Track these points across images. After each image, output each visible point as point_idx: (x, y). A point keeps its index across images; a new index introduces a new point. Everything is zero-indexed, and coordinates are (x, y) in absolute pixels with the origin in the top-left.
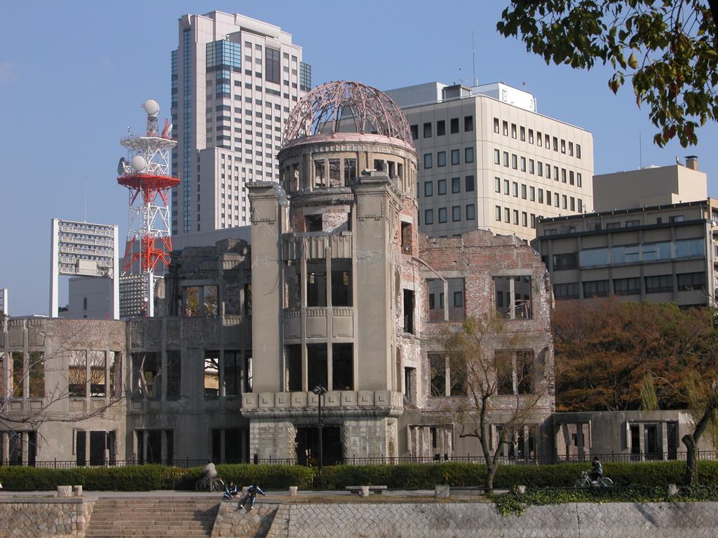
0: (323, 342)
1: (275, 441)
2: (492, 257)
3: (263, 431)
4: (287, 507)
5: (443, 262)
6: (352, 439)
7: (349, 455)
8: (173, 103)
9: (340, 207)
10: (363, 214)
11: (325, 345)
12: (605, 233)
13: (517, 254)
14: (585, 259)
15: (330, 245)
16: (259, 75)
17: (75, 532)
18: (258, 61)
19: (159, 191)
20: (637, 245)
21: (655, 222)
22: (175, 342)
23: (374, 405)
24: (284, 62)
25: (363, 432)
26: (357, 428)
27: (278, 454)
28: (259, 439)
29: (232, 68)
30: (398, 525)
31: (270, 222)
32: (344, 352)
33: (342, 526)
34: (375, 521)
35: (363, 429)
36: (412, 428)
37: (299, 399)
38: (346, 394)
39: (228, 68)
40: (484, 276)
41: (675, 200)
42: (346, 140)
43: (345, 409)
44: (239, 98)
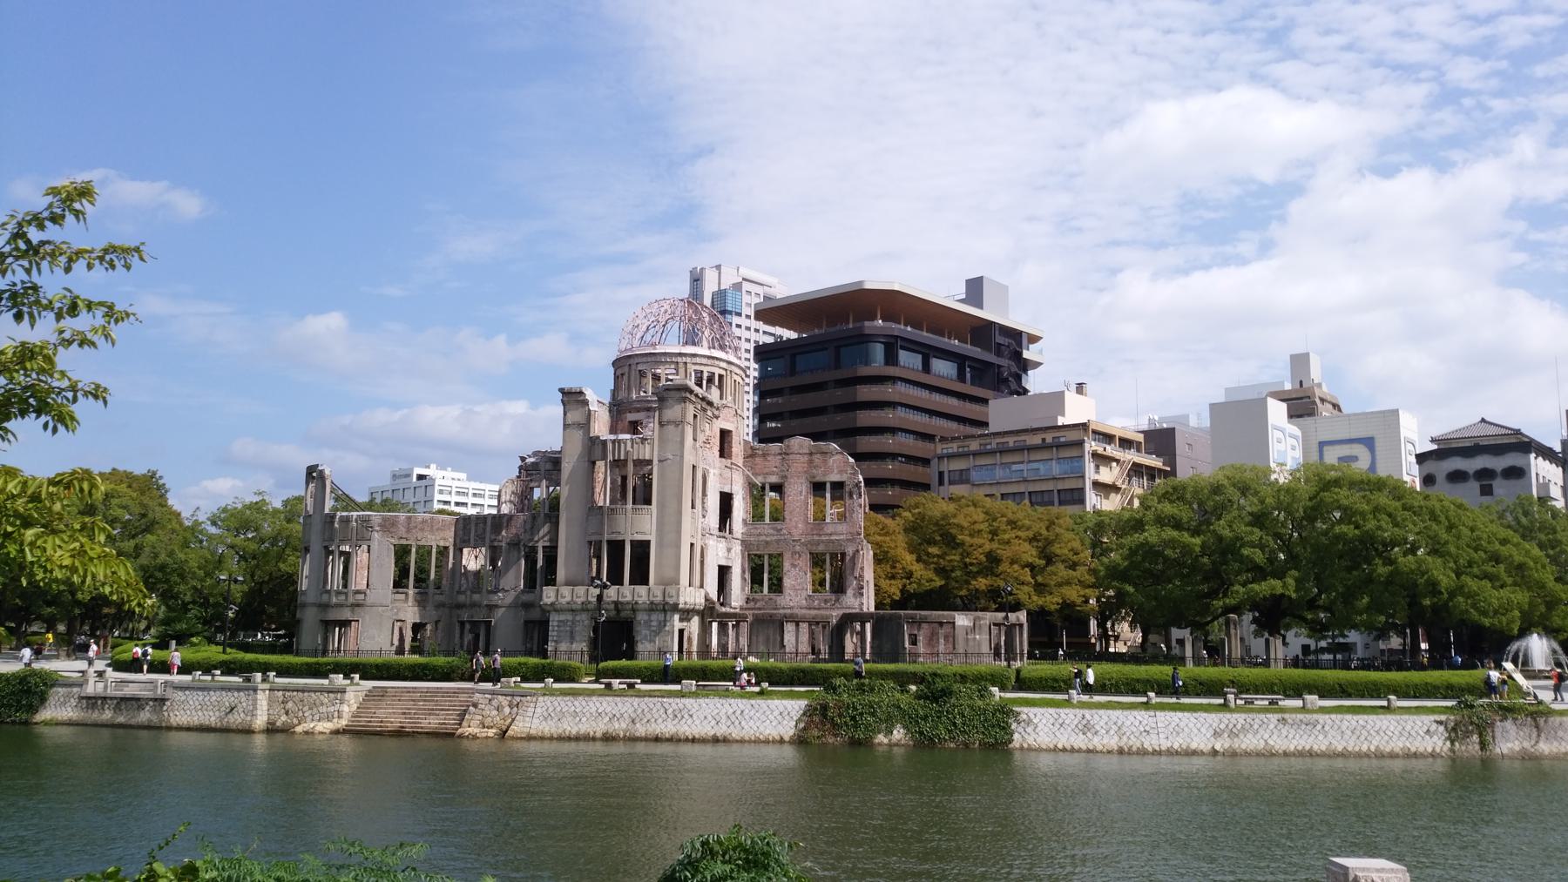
1: (572, 633)
2: (811, 462)
4: (534, 699)
6: (644, 632)
12: (992, 453)
15: (632, 447)
17: (336, 720)
20: (1022, 462)
21: (1040, 442)
26: (648, 623)
32: (641, 549)
35: (654, 623)
36: (711, 623)
39: (730, 313)
41: (1061, 421)
43: (636, 603)
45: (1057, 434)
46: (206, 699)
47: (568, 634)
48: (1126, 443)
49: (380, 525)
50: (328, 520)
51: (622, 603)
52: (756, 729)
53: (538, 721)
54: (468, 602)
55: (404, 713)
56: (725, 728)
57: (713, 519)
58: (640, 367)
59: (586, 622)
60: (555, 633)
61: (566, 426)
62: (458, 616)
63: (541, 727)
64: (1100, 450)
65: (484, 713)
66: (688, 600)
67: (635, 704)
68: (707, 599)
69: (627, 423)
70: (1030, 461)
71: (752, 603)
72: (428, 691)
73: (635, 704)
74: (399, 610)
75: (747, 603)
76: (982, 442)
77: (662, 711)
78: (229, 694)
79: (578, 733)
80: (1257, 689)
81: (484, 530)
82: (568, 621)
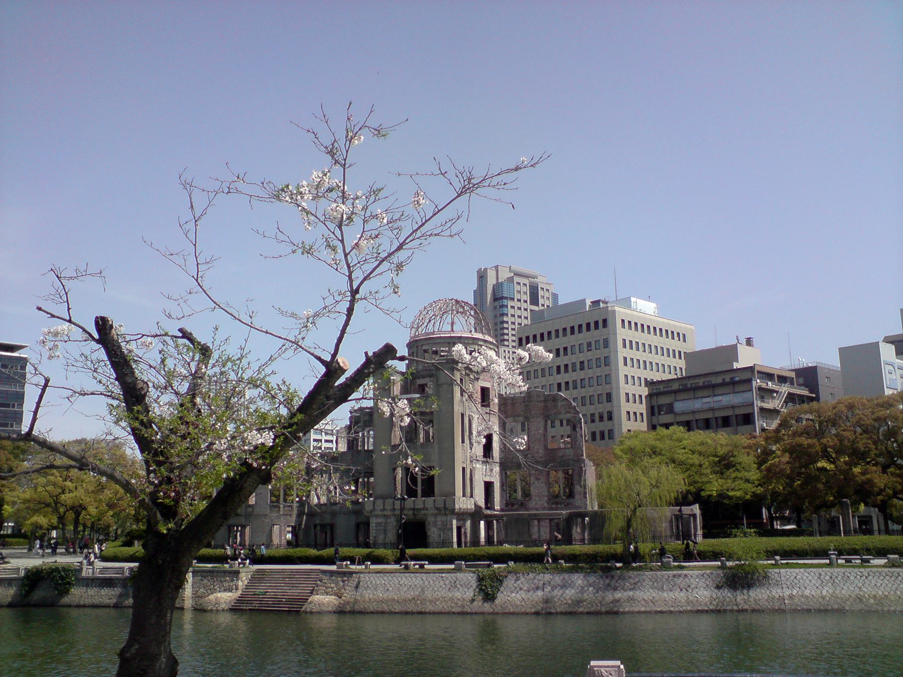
7: (431, 540)
13: (562, 406)
14: (679, 406)
16: (526, 301)
24: (541, 293)
26: (435, 524)
27: (387, 539)
28: (376, 530)
30: (426, 589)
33: (390, 589)
35: (439, 523)
39: (506, 298)
40: (540, 420)
41: (736, 366)
43: (427, 509)
44: (513, 316)
45: (732, 375)
47: (383, 531)
48: (783, 379)
57: (479, 450)
58: (425, 347)
64: (764, 385)
66: (461, 506)
68: (476, 505)
69: (417, 386)
70: (714, 396)
72: (292, 571)
73: (424, 578)
75: (506, 506)
77: (442, 583)
80: (855, 552)
82: (382, 523)
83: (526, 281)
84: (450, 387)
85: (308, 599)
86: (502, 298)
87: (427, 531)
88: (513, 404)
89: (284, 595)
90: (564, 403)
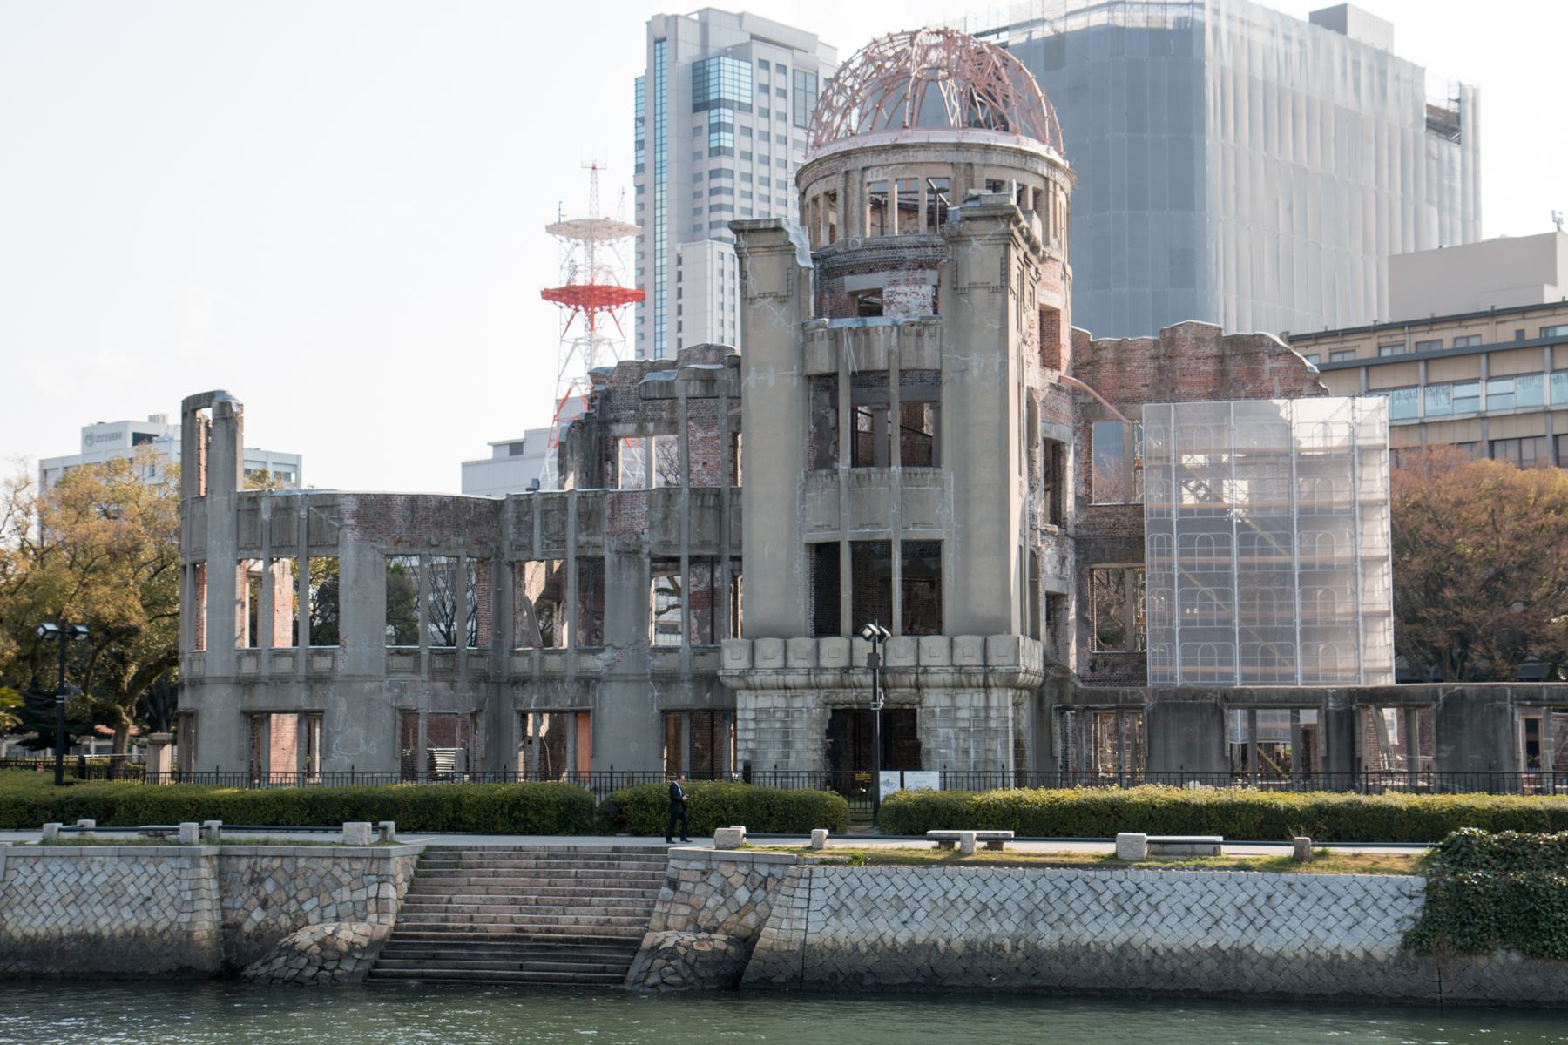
0: (882, 537)
3: (764, 716)
5: (1122, 387)
6: (941, 731)
8: (637, 166)
9: (918, 274)
10: (964, 283)
11: (887, 544)
13: (1273, 371)
17: (373, 918)
18: (782, 93)
19: (610, 311)
20: (1475, 381)
22: (598, 539)
23: (985, 666)
25: (963, 719)
27: (792, 760)
29: (736, 106)
31: (781, 300)
34: (990, 904)
37: (834, 649)
38: (928, 641)
39: (730, 104)
41: (1551, 296)
42: (932, 140)
43: (926, 671)
45: (1550, 321)
46: (84, 881)
47: (778, 736)
49: (356, 515)
50: (245, 505)
51: (893, 670)
52: (1306, 935)
53: (820, 917)
54: (536, 673)
55: (515, 902)
56: (1234, 934)
59: (816, 712)
60: (750, 735)
61: (747, 299)
62: (516, 701)
63: (829, 930)
65: (693, 901)
67: (1027, 882)
69: (845, 296)
70: (1490, 379)
71: (1107, 671)
73: (1027, 882)
74: (403, 689)
75: (1093, 669)
76: (1383, 340)
77: (1088, 897)
78: (138, 870)
79: (911, 942)
81: (564, 525)
82: (776, 709)
83: (782, 57)
84: (999, 297)
85: (639, 943)
86: (719, 103)
87: (921, 735)
88: (1119, 363)
89: (549, 931)
90: (1281, 363)
